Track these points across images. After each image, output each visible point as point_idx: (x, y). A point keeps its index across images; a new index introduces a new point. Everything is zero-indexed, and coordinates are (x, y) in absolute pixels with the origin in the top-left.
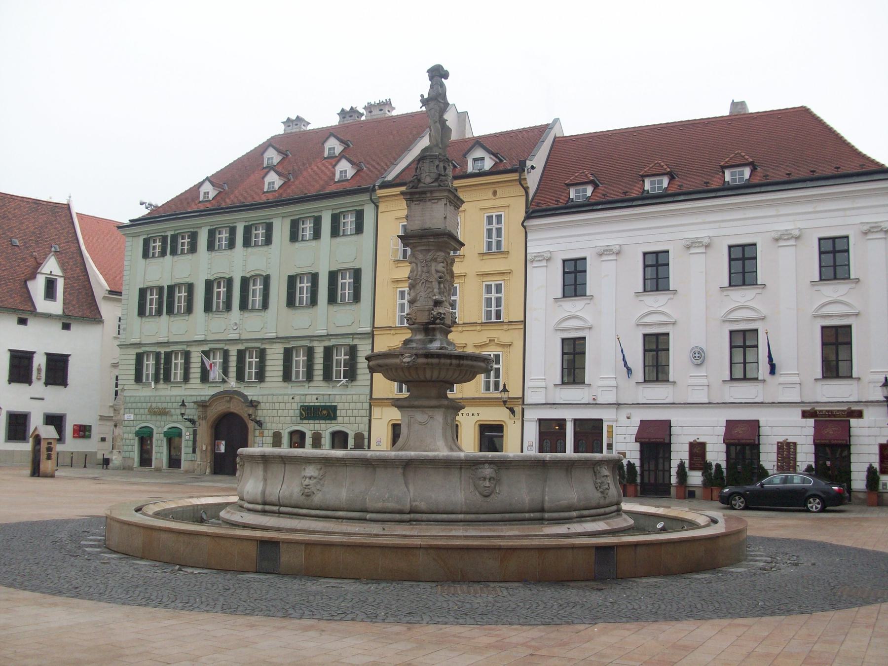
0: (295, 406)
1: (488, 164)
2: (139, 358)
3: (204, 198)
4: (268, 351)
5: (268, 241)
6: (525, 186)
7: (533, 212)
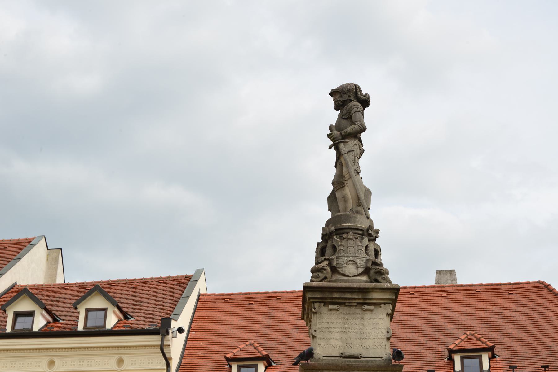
1: (112, 321)
6: (167, 355)
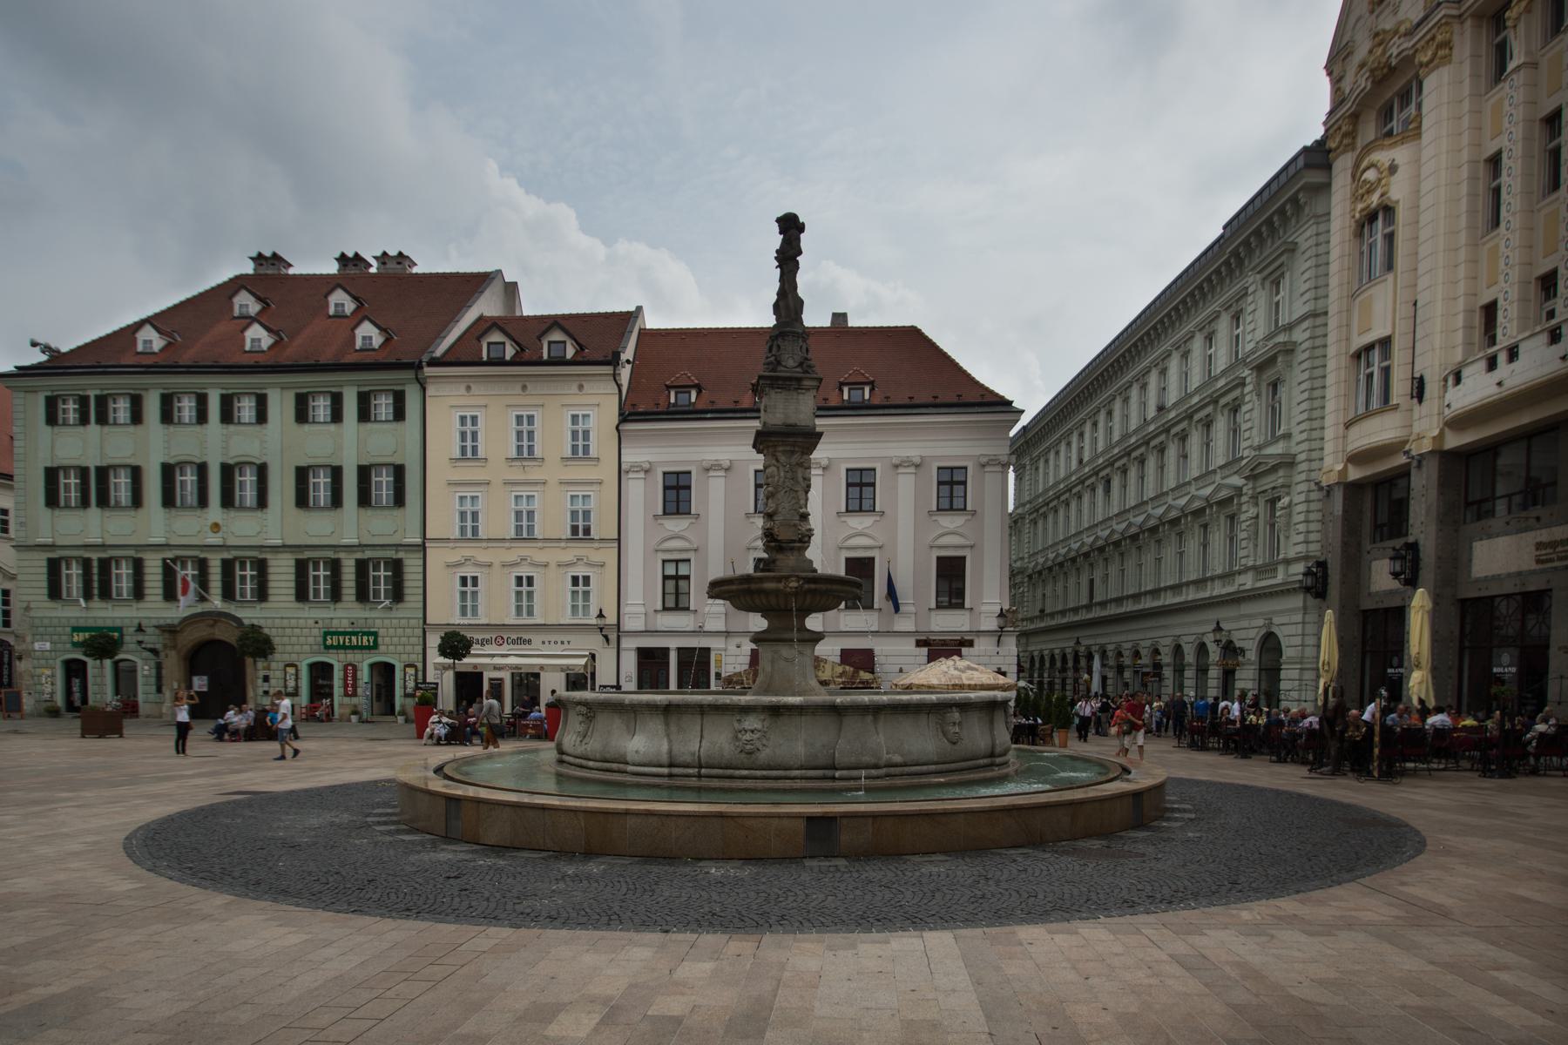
0: (315, 632)
2: (54, 567)
4: (271, 563)
5: (262, 417)
7: (630, 414)
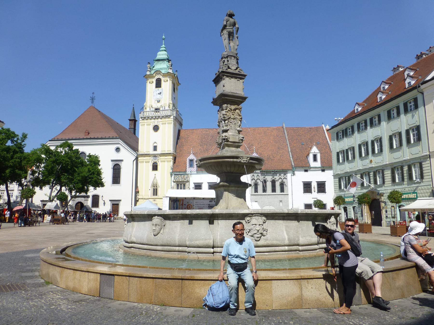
3: (357, 111)
